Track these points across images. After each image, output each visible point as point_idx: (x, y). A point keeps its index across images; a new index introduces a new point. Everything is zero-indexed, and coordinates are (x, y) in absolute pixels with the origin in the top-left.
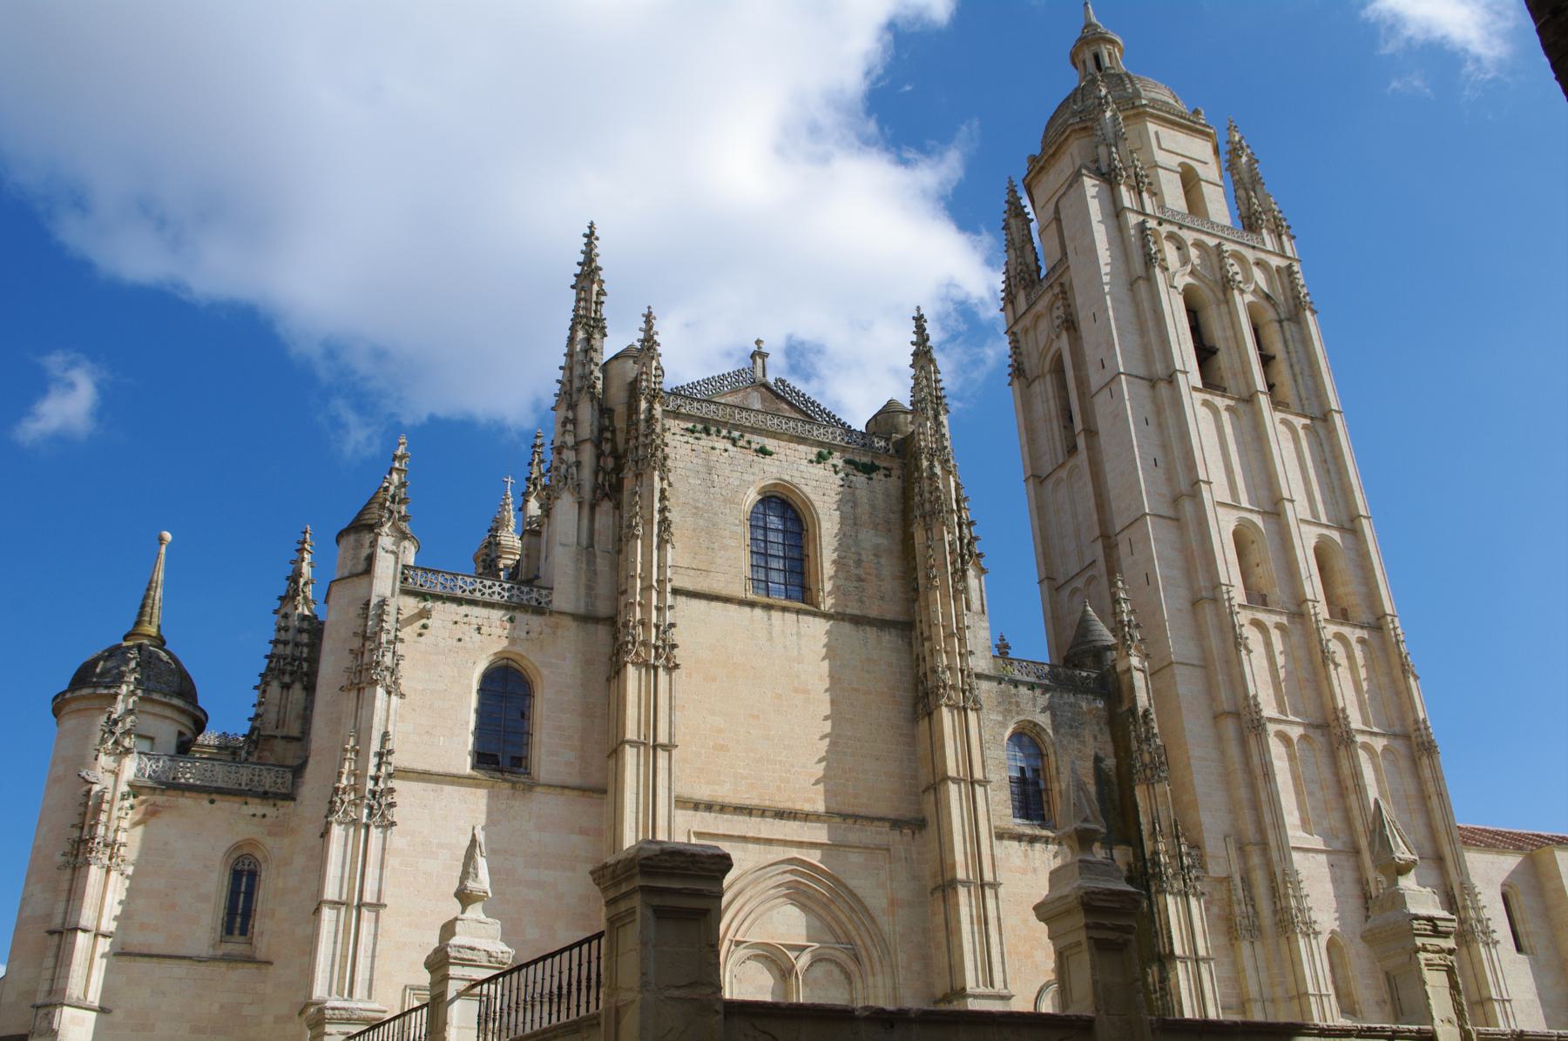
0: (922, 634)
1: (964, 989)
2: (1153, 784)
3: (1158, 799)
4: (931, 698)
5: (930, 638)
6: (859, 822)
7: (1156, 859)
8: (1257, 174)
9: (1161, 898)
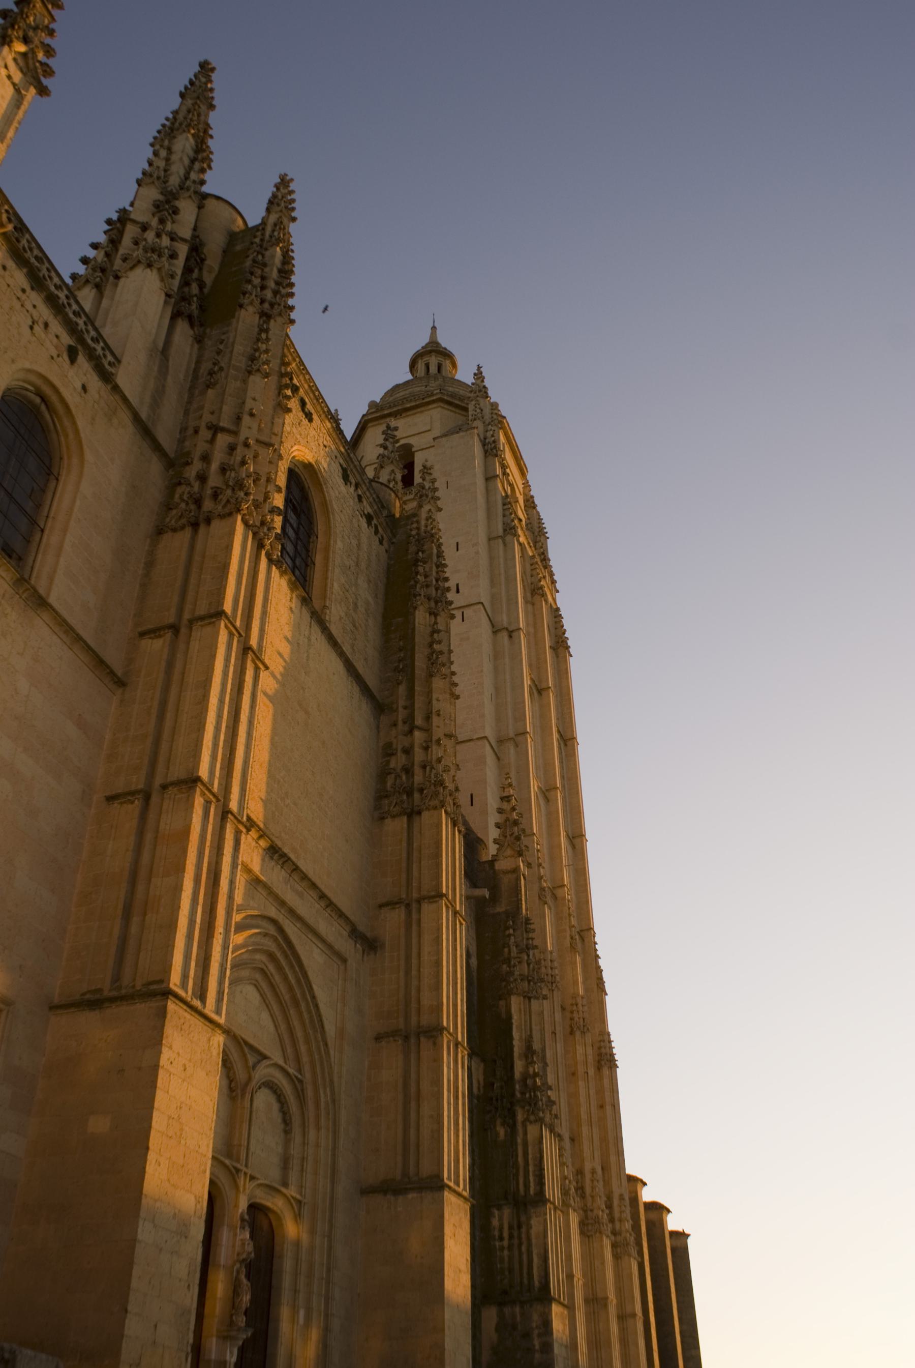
0: (410, 719)
1: (439, 1177)
2: (529, 998)
3: (533, 1017)
4: (416, 795)
5: (427, 730)
6: (329, 910)
7: (529, 1082)
8: (545, 528)
9: (532, 1130)
